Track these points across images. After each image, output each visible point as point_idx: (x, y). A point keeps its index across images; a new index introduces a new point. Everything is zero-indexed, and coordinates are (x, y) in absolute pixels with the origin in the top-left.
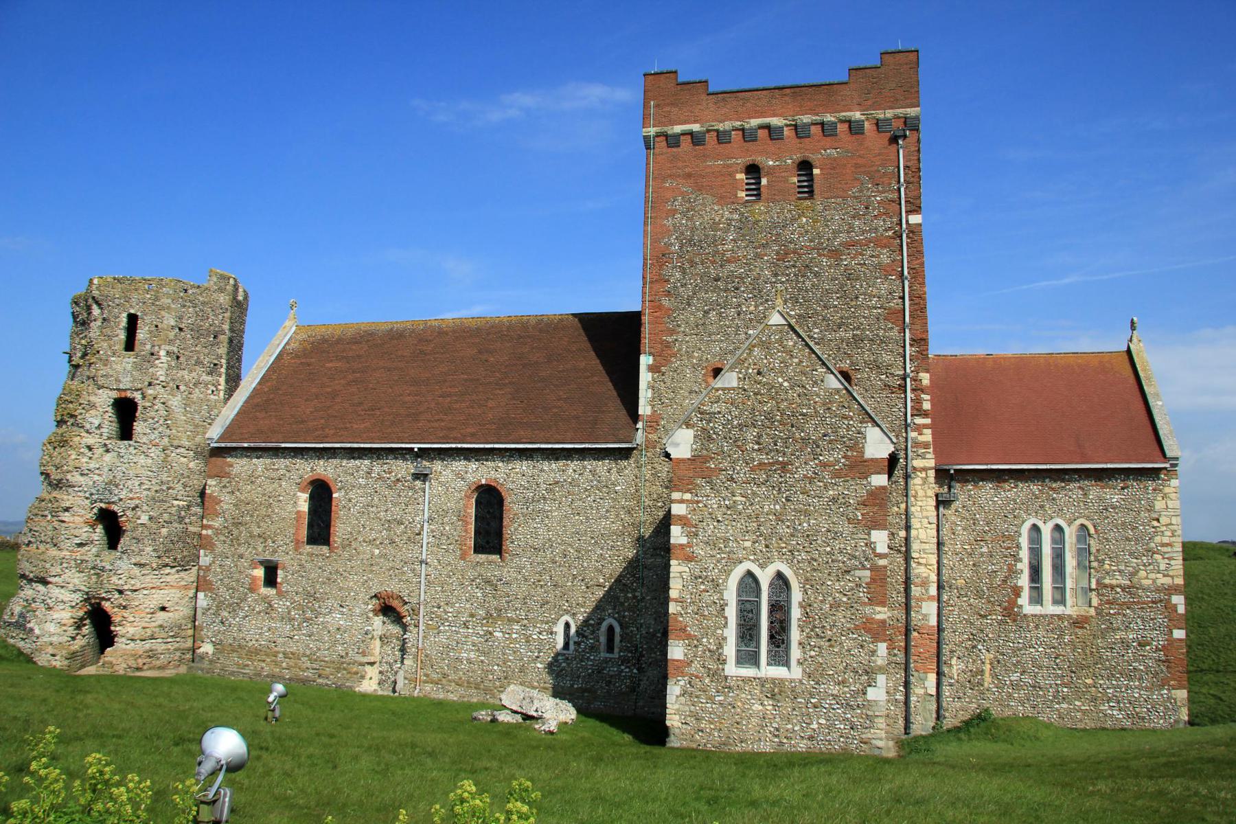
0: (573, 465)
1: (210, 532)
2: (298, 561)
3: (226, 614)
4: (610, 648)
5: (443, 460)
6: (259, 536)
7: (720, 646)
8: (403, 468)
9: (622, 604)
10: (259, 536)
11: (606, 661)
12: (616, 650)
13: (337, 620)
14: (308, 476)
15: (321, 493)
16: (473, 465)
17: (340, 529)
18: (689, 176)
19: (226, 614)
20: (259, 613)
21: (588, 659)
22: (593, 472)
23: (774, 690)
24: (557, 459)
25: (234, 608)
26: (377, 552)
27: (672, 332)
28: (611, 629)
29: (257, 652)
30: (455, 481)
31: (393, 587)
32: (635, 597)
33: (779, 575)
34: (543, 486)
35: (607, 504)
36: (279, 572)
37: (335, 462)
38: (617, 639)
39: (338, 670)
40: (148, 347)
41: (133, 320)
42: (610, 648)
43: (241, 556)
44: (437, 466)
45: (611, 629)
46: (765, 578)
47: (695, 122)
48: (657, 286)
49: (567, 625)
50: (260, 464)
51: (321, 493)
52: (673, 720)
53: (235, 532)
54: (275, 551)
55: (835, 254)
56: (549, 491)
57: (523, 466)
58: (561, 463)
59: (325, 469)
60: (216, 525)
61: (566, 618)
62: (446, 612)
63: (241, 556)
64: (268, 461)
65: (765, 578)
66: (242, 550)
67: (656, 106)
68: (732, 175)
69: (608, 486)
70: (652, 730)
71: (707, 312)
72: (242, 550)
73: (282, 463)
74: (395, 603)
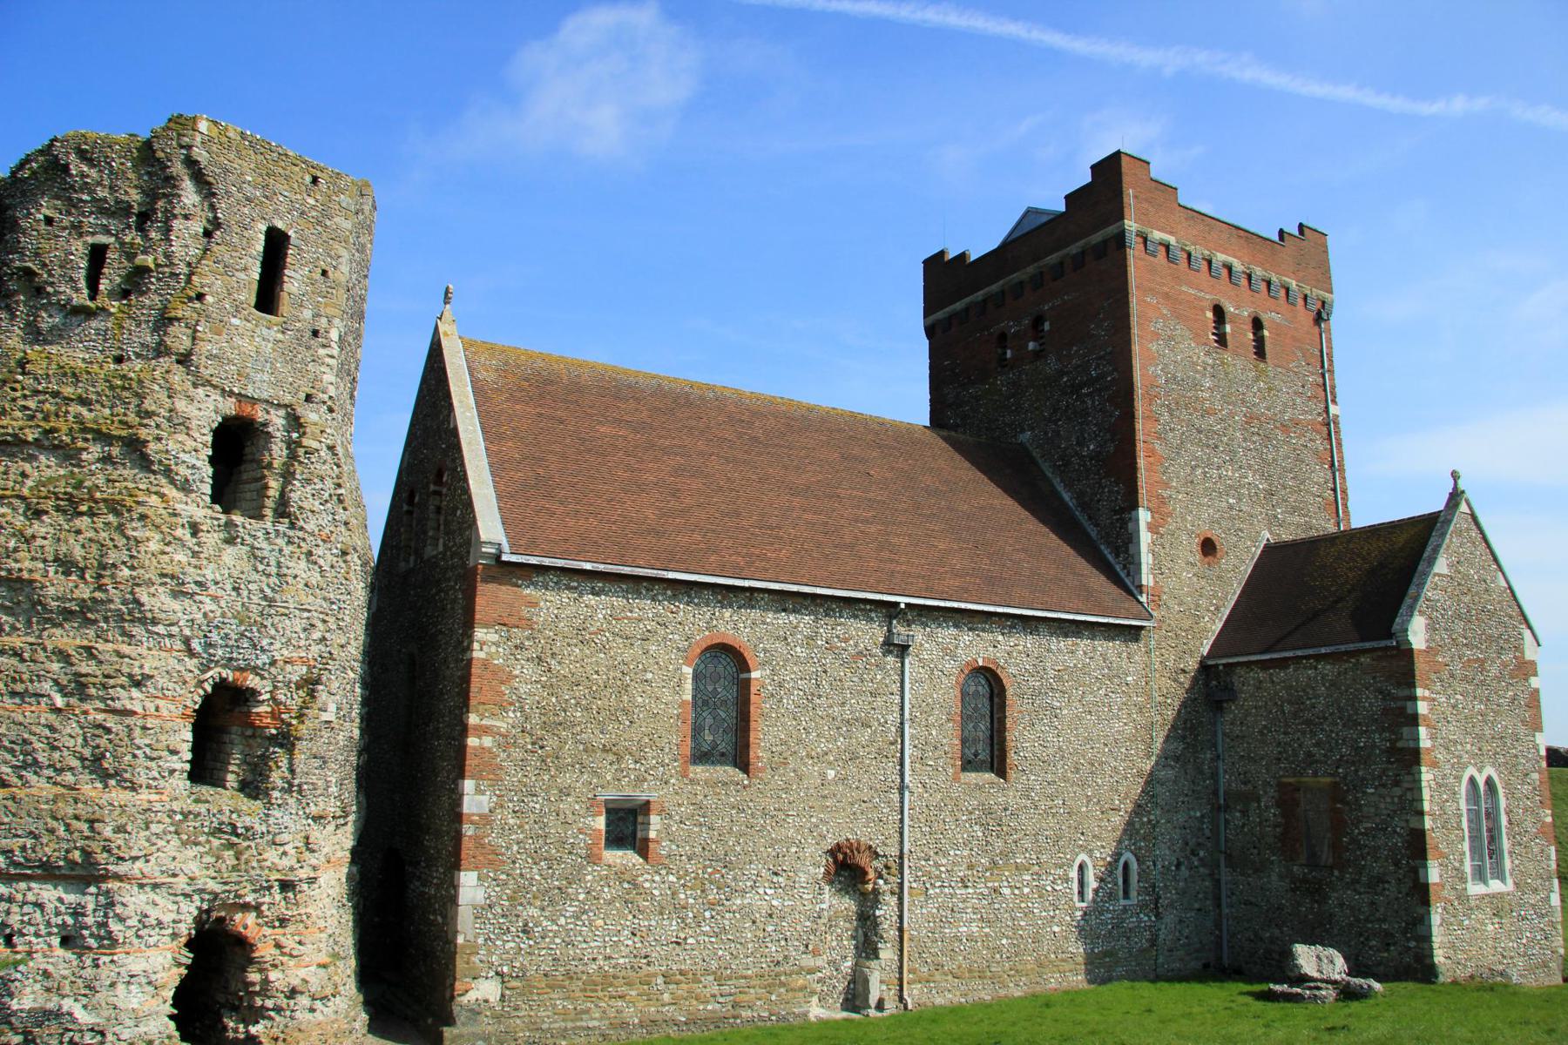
0: (1084, 644)
1: (487, 741)
2: (679, 796)
3: (535, 912)
4: (1126, 895)
5: (925, 625)
6: (605, 750)
7: (1461, 862)
8: (869, 633)
9: (1138, 832)
10: (605, 750)
11: (1125, 910)
12: (1133, 894)
13: (765, 898)
14: (702, 638)
15: (725, 664)
16: (967, 637)
17: (764, 738)
18: (1166, 296)
19: (535, 912)
20: (610, 903)
21: (1108, 910)
22: (1104, 657)
23: (1498, 906)
24: (1066, 636)
25: (553, 898)
26: (831, 774)
27: (1167, 486)
28: (1126, 866)
29: (607, 980)
30: (943, 656)
31: (862, 832)
32: (1150, 821)
33: (1489, 782)
34: (1052, 673)
35: (1118, 699)
36: (654, 819)
37: (755, 614)
38: (1134, 878)
39: (770, 989)
40: (307, 314)
41: (276, 244)
42: (1126, 895)
43: (564, 792)
44: (918, 635)
45: (1126, 866)
46: (1481, 781)
47: (1171, 233)
48: (1149, 425)
49: (1081, 868)
50: (599, 606)
51: (725, 664)
52: (1439, 957)
53: (551, 743)
54: (640, 780)
55: (1284, 428)
56: (1059, 679)
57: (1027, 642)
58: (1070, 641)
59: (734, 625)
60: (502, 725)
61: (1082, 857)
62: (937, 865)
63: (564, 792)
64: (618, 602)
65: (1481, 781)
66: (567, 779)
67: (1135, 197)
68: (1203, 310)
69: (1115, 675)
70: (1424, 971)
71: (1193, 468)
72: (567, 779)
73: (645, 609)
74: (863, 860)
